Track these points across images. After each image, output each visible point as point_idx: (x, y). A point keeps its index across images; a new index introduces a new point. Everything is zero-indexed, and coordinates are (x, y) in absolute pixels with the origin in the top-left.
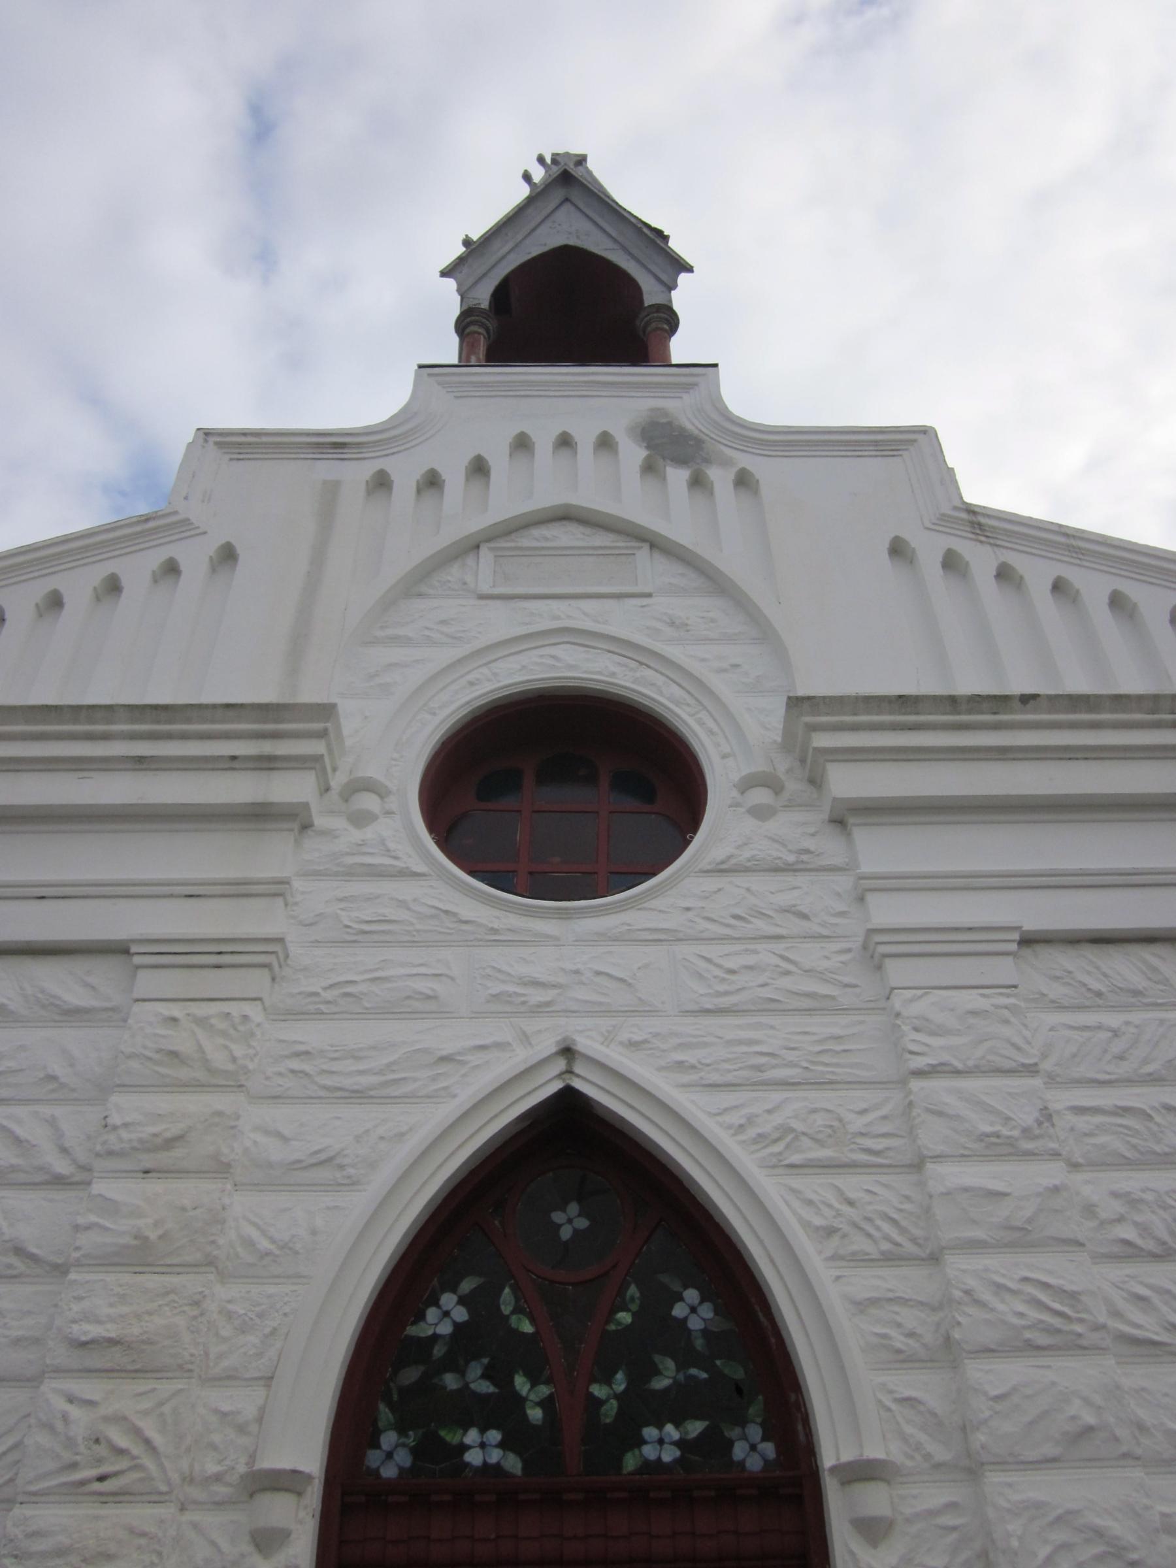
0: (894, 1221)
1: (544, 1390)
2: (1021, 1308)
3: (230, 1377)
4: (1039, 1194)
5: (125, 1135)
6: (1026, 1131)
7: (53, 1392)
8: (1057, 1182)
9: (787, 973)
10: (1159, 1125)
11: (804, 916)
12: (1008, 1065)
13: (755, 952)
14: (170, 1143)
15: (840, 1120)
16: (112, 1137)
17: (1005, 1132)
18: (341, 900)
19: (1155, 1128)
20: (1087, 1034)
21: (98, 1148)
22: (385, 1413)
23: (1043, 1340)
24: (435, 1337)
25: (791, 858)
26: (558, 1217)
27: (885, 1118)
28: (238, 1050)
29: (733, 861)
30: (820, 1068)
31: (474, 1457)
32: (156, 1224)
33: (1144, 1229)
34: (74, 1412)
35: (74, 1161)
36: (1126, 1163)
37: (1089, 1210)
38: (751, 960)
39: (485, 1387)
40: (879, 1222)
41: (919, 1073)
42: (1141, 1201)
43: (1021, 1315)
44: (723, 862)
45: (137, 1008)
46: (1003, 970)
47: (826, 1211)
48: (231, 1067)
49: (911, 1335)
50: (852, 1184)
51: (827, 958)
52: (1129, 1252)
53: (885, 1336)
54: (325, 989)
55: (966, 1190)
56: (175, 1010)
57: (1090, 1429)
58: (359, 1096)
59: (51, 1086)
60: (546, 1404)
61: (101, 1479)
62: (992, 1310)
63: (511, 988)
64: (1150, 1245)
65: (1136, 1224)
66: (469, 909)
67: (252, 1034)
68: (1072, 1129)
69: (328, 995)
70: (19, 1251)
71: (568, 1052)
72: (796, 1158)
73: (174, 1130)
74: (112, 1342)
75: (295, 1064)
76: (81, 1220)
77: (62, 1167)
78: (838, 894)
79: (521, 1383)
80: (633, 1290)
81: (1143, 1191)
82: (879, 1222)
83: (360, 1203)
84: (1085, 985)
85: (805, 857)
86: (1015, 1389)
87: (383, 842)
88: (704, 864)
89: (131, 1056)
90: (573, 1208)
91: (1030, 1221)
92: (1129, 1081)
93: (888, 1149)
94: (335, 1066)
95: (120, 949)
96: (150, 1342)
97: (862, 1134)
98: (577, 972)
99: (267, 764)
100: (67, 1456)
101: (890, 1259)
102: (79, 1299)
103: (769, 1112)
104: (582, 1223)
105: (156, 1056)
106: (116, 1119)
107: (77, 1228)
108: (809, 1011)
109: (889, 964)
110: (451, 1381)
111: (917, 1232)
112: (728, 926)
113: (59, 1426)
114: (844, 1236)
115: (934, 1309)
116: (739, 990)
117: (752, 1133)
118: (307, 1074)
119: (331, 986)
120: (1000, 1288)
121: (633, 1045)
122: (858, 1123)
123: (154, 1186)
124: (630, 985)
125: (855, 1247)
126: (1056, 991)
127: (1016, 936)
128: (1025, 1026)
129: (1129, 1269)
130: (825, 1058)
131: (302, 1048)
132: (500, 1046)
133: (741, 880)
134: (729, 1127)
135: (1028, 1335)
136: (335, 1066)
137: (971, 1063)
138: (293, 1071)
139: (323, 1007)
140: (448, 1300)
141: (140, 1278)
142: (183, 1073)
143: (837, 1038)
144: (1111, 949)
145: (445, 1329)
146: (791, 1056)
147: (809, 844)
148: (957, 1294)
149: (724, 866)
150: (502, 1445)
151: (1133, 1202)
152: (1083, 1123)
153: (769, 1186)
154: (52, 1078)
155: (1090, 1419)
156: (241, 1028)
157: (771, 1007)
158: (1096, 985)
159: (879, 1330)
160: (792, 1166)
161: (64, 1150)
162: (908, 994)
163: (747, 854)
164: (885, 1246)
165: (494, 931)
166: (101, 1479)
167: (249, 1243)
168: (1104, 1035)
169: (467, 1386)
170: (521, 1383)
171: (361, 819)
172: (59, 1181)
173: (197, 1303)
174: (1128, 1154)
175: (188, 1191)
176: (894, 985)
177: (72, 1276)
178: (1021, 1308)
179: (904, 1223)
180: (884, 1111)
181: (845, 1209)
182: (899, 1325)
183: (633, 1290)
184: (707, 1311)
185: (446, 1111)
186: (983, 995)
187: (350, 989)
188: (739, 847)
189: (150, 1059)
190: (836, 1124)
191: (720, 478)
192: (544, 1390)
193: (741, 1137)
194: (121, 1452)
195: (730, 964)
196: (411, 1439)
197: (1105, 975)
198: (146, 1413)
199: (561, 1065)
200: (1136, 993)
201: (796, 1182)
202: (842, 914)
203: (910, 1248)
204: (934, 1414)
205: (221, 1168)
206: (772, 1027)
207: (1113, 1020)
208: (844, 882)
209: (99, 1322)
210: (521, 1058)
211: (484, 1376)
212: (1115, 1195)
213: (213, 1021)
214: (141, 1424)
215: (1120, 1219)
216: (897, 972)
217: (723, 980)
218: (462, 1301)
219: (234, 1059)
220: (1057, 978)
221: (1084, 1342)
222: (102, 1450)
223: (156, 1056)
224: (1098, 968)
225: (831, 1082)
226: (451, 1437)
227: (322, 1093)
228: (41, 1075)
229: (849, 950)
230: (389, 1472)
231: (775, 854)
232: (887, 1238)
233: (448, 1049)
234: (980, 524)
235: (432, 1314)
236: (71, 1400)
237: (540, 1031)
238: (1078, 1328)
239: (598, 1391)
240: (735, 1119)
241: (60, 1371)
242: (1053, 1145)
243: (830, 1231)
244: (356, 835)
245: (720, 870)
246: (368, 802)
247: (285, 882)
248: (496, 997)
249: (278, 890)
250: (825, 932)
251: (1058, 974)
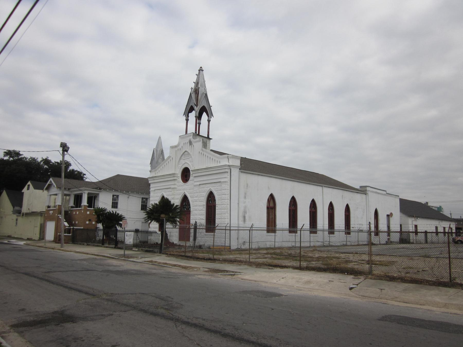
46: (198, 187)
92: (202, 193)
99: (174, 177)
171: (179, 179)
185: (180, 196)
191: (192, 146)
234: (203, 150)
244: (178, 180)
245: (190, 181)
246: (179, 178)
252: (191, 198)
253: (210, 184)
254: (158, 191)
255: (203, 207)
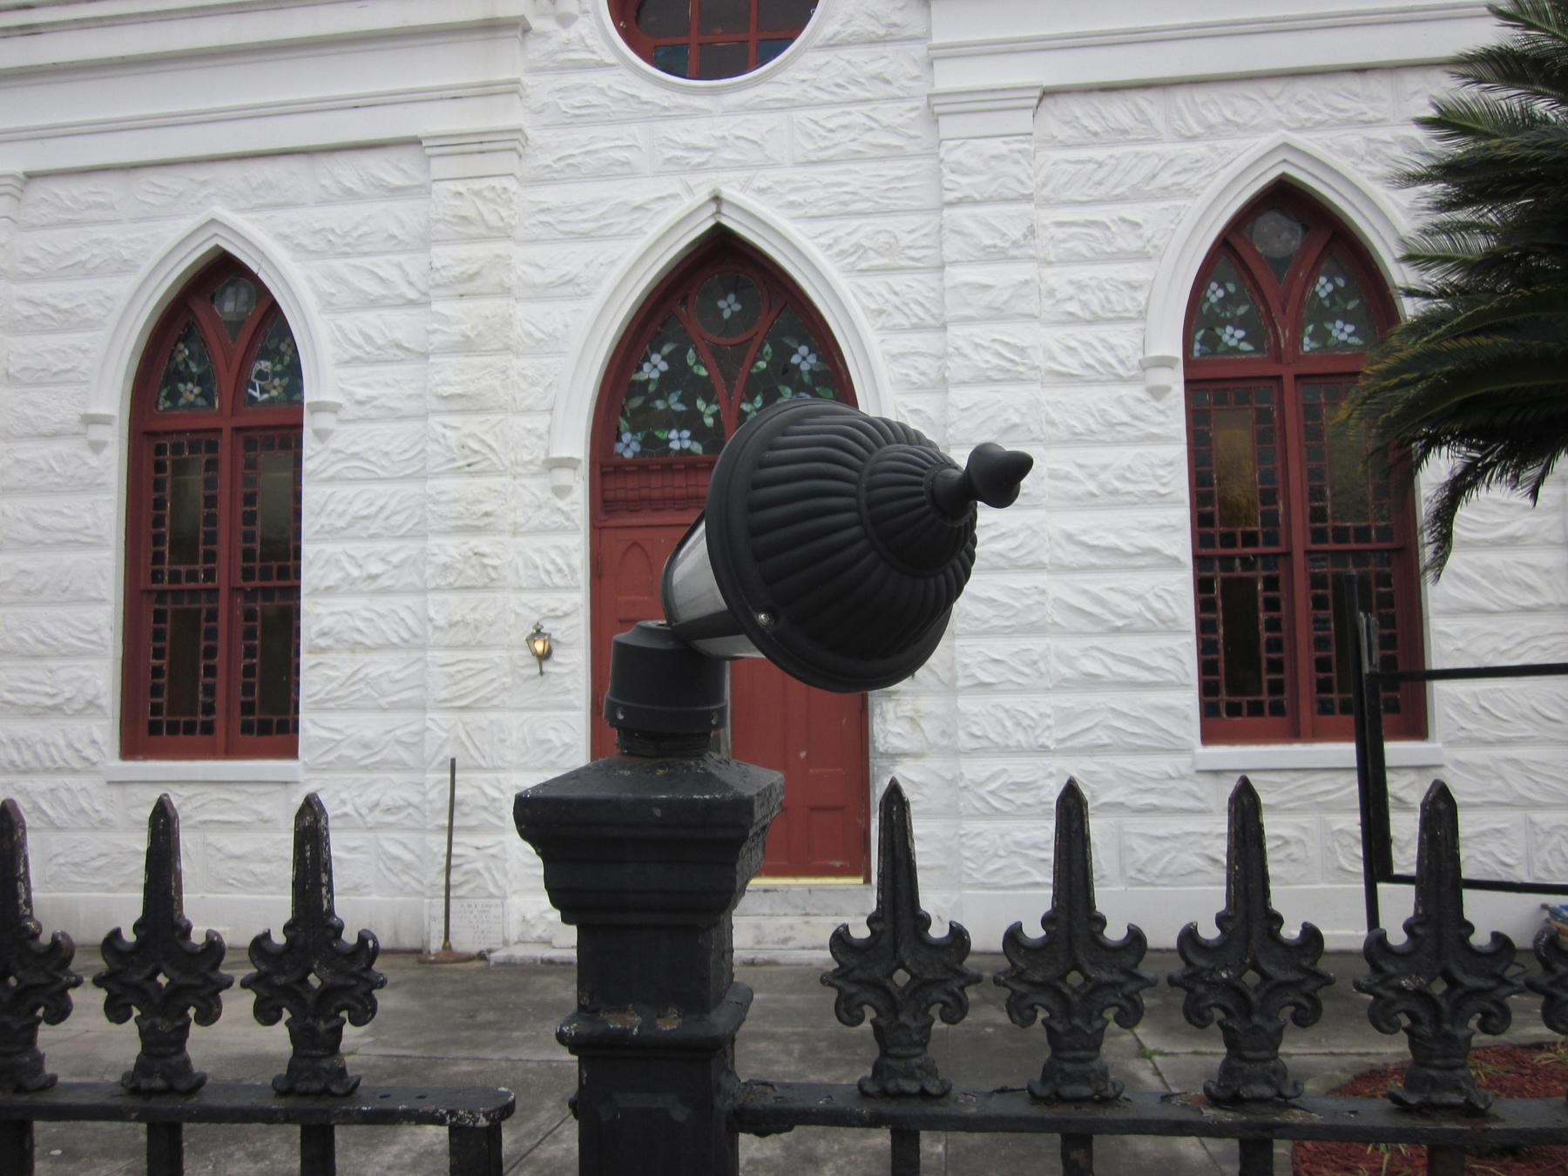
0: (922, 305)
1: (714, 408)
2: (988, 357)
3: (529, 411)
4: (1014, 286)
5: (444, 273)
6: (1015, 244)
7: (433, 421)
8: (1027, 277)
9: (871, 129)
10: (1113, 233)
11: (887, 82)
12: (1011, 195)
13: (849, 113)
14: (472, 277)
15: (896, 238)
16: (437, 276)
17: (1000, 244)
18: (559, 90)
19: (1109, 234)
20: (1079, 166)
21: (431, 283)
22: (624, 424)
23: (997, 375)
24: (649, 381)
25: (882, 32)
26: (722, 304)
27: (926, 235)
28: (504, 212)
29: (839, 37)
30: (886, 201)
31: (675, 445)
32: (473, 328)
33: (1085, 305)
34: (448, 433)
35: (418, 290)
36: (1084, 260)
37: (1051, 293)
38: (845, 120)
39: (680, 407)
40: (912, 306)
41: (950, 204)
42: (1086, 286)
43: (987, 362)
44: (831, 39)
45: (435, 186)
46: (1023, 121)
47: (878, 298)
48: (501, 224)
49: (922, 373)
50: (898, 281)
51: (901, 115)
52: (1073, 319)
53: (907, 375)
54: (555, 162)
55: (967, 284)
56: (459, 187)
57: (1014, 426)
58: (584, 236)
59: (394, 242)
60: (715, 416)
61: (469, 465)
62: (969, 359)
63: (679, 153)
64: (1087, 315)
65: (1080, 301)
66: (649, 93)
67: (511, 201)
68: (1052, 238)
69: (557, 166)
70: (399, 346)
71: (717, 199)
72: (864, 265)
73: (473, 268)
74: (461, 396)
75: (542, 218)
76: (429, 328)
77: (412, 295)
78: (915, 61)
79: (700, 404)
80: (768, 348)
81: (1091, 279)
82: (912, 306)
83: (592, 306)
84: (1086, 127)
85: (893, 30)
86: (975, 405)
87: (582, 39)
88: (817, 42)
89: (438, 221)
90: (731, 298)
91: (1005, 303)
93: (925, 257)
94: (566, 217)
95: (415, 142)
96: (480, 394)
97: (909, 247)
98: (724, 138)
100: (449, 455)
101: (915, 328)
102: (439, 372)
103: (849, 234)
104: (737, 307)
105: (454, 220)
106: (437, 264)
107: (428, 332)
108: (883, 158)
109: (941, 119)
110: (660, 405)
111: (936, 311)
112: (831, 93)
113: (442, 440)
114: (889, 315)
115: (939, 358)
116: (835, 145)
117: (837, 249)
118: (551, 224)
119: (560, 159)
120: (977, 346)
121: (761, 191)
122: (907, 240)
123: (467, 304)
124: (760, 146)
125: (895, 322)
126: (1065, 133)
127: (1038, 93)
128: (1030, 165)
129: (1070, 330)
130: (890, 194)
131: (545, 206)
132: (674, 196)
133: (844, 53)
134: (822, 246)
135: (989, 373)
136: (566, 217)
137: (986, 195)
138: (541, 223)
139: (555, 175)
140: (656, 358)
141: (468, 359)
142: (472, 230)
143: (900, 179)
144: (1114, 96)
145: (655, 375)
146: (867, 193)
147: (896, 18)
148: (951, 350)
149: (832, 42)
150: (691, 438)
151: (1081, 286)
152: (1060, 233)
153: (843, 284)
154: (393, 237)
155: (1016, 419)
156: (504, 197)
157: (857, 157)
158: (1095, 127)
159: (905, 371)
160: (861, 271)
161: (411, 284)
162: (951, 144)
163: (850, 30)
164: (915, 320)
165: (665, 109)
166: (469, 465)
167: (530, 335)
168: (1091, 167)
169: (669, 407)
170: (700, 404)
172: (412, 303)
173: (504, 372)
174: (1087, 254)
175: (489, 306)
176: (942, 136)
177: (432, 360)
178: (988, 357)
179: (928, 305)
180: (926, 230)
181: (892, 297)
182: (916, 368)
183: (768, 348)
184: (812, 359)
185: (639, 245)
186: (1004, 142)
187: (571, 161)
188: (843, 25)
189: (449, 222)
190: (892, 240)
192: (714, 408)
193: (830, 253)
194: (476, 452)
195: (831, 125)
196: (639, 436)
197: (1104, 118)
198: (486, 432)
199: (713, 208)
200: (1124, 132)
201: (863, 281)
202: (916, 78)
203: (930, 321)
204: (929, 418)
205: (505, 291)
206: (857, 172)
207: (1100, 154)
208: (919, 50)
209: (451, 385)
210: (688, 203)
211: (680, 401)
212: (1071, 282)
213: (485, 193)
214: (485, 437)
215: (1071, 298)
216: (948, 126)
217: (825, 138)
218: (664, 358)
219: (502, 219)
220: (1066, 123)
221: (1024, 377)
222: (466, 451)
223: (454, 220)
224: (1100, 113)
225: (893, 211)
226: (661, 435)
227: (561, 236)
228: (385, 235)
229: (917, 108)
230: (628, 455)
231: (871, 28)
232: (916, 315)
233: (638, 200)
235: (646, 367)
236: (445, 426)
237: (699, 184)
238: (1021, 369)
239: (746, 407)
240: (825, 240)
241: (434, 412)
242: (1032, 252)
243: (881, 312)
244: (565, 34)
245: (830, 45)
247: (516, 82)
248: (669, 161)
249: (512, 89)
250: (901, 94)
251: (1068, 118)
252: (852, 270)
253: (1273, 88)
254: (109, 187)
255: (1138, 391)
